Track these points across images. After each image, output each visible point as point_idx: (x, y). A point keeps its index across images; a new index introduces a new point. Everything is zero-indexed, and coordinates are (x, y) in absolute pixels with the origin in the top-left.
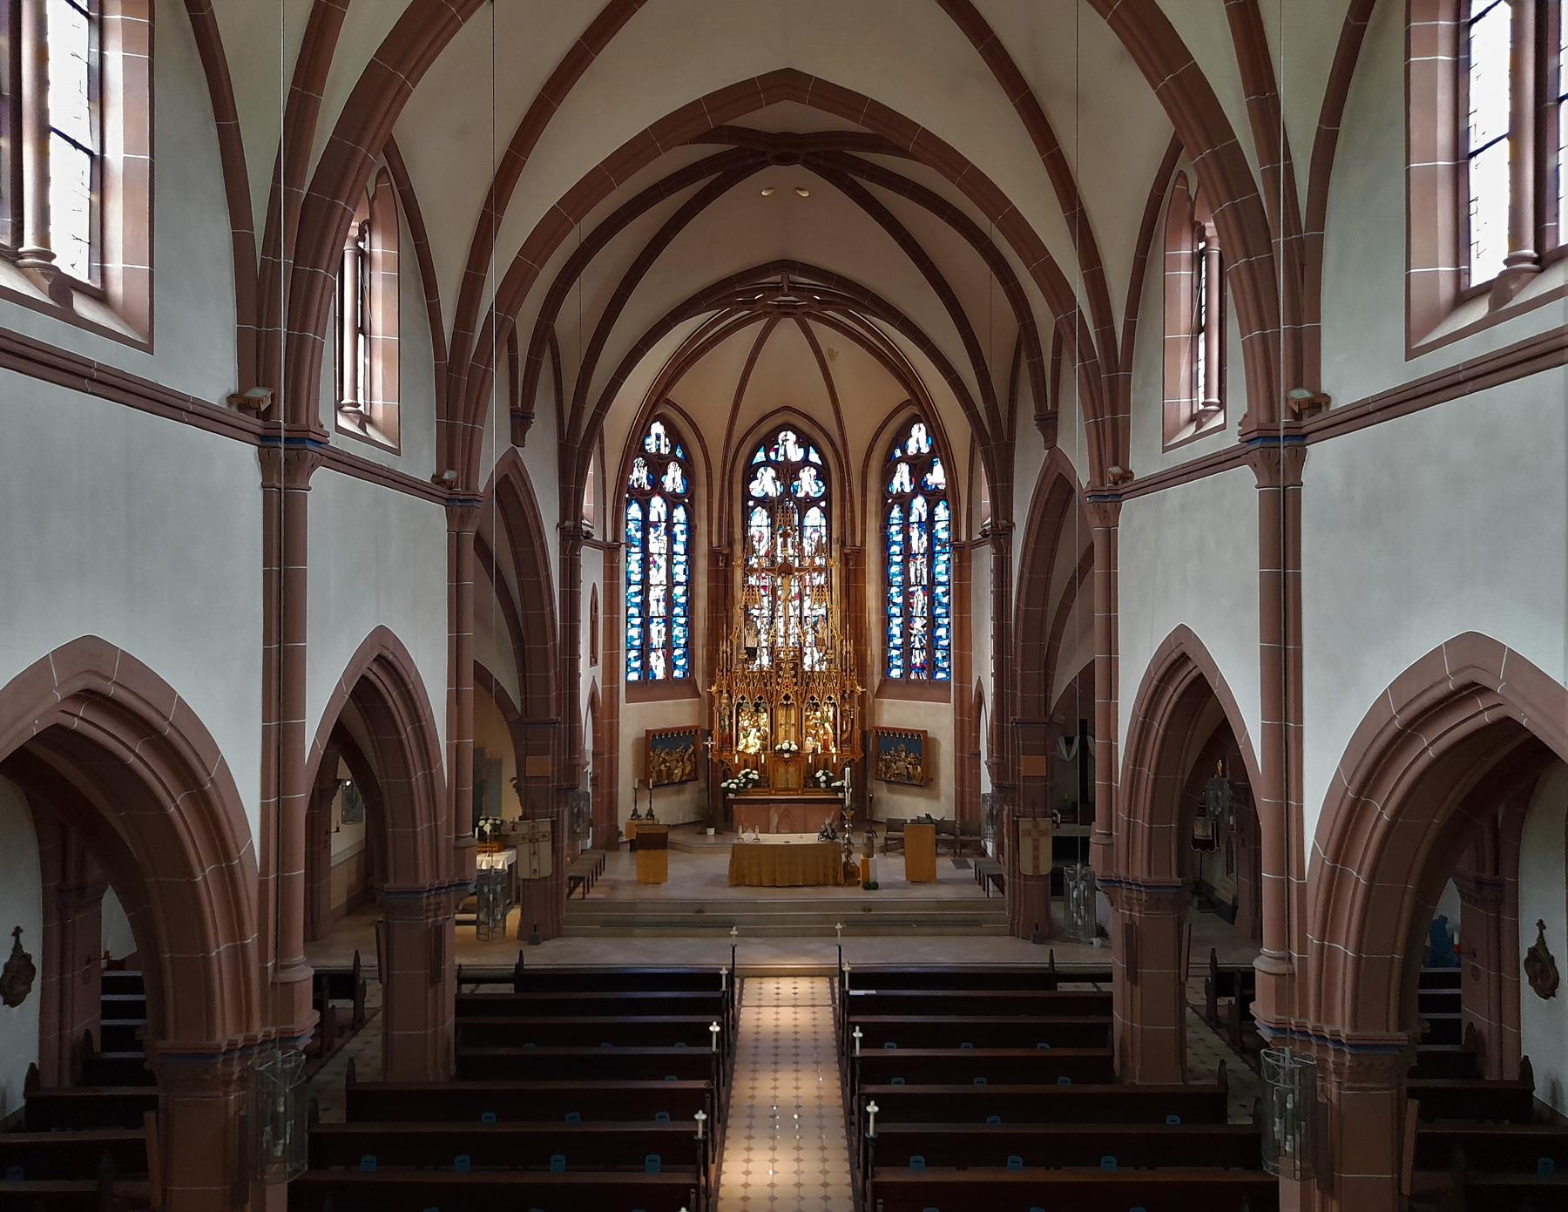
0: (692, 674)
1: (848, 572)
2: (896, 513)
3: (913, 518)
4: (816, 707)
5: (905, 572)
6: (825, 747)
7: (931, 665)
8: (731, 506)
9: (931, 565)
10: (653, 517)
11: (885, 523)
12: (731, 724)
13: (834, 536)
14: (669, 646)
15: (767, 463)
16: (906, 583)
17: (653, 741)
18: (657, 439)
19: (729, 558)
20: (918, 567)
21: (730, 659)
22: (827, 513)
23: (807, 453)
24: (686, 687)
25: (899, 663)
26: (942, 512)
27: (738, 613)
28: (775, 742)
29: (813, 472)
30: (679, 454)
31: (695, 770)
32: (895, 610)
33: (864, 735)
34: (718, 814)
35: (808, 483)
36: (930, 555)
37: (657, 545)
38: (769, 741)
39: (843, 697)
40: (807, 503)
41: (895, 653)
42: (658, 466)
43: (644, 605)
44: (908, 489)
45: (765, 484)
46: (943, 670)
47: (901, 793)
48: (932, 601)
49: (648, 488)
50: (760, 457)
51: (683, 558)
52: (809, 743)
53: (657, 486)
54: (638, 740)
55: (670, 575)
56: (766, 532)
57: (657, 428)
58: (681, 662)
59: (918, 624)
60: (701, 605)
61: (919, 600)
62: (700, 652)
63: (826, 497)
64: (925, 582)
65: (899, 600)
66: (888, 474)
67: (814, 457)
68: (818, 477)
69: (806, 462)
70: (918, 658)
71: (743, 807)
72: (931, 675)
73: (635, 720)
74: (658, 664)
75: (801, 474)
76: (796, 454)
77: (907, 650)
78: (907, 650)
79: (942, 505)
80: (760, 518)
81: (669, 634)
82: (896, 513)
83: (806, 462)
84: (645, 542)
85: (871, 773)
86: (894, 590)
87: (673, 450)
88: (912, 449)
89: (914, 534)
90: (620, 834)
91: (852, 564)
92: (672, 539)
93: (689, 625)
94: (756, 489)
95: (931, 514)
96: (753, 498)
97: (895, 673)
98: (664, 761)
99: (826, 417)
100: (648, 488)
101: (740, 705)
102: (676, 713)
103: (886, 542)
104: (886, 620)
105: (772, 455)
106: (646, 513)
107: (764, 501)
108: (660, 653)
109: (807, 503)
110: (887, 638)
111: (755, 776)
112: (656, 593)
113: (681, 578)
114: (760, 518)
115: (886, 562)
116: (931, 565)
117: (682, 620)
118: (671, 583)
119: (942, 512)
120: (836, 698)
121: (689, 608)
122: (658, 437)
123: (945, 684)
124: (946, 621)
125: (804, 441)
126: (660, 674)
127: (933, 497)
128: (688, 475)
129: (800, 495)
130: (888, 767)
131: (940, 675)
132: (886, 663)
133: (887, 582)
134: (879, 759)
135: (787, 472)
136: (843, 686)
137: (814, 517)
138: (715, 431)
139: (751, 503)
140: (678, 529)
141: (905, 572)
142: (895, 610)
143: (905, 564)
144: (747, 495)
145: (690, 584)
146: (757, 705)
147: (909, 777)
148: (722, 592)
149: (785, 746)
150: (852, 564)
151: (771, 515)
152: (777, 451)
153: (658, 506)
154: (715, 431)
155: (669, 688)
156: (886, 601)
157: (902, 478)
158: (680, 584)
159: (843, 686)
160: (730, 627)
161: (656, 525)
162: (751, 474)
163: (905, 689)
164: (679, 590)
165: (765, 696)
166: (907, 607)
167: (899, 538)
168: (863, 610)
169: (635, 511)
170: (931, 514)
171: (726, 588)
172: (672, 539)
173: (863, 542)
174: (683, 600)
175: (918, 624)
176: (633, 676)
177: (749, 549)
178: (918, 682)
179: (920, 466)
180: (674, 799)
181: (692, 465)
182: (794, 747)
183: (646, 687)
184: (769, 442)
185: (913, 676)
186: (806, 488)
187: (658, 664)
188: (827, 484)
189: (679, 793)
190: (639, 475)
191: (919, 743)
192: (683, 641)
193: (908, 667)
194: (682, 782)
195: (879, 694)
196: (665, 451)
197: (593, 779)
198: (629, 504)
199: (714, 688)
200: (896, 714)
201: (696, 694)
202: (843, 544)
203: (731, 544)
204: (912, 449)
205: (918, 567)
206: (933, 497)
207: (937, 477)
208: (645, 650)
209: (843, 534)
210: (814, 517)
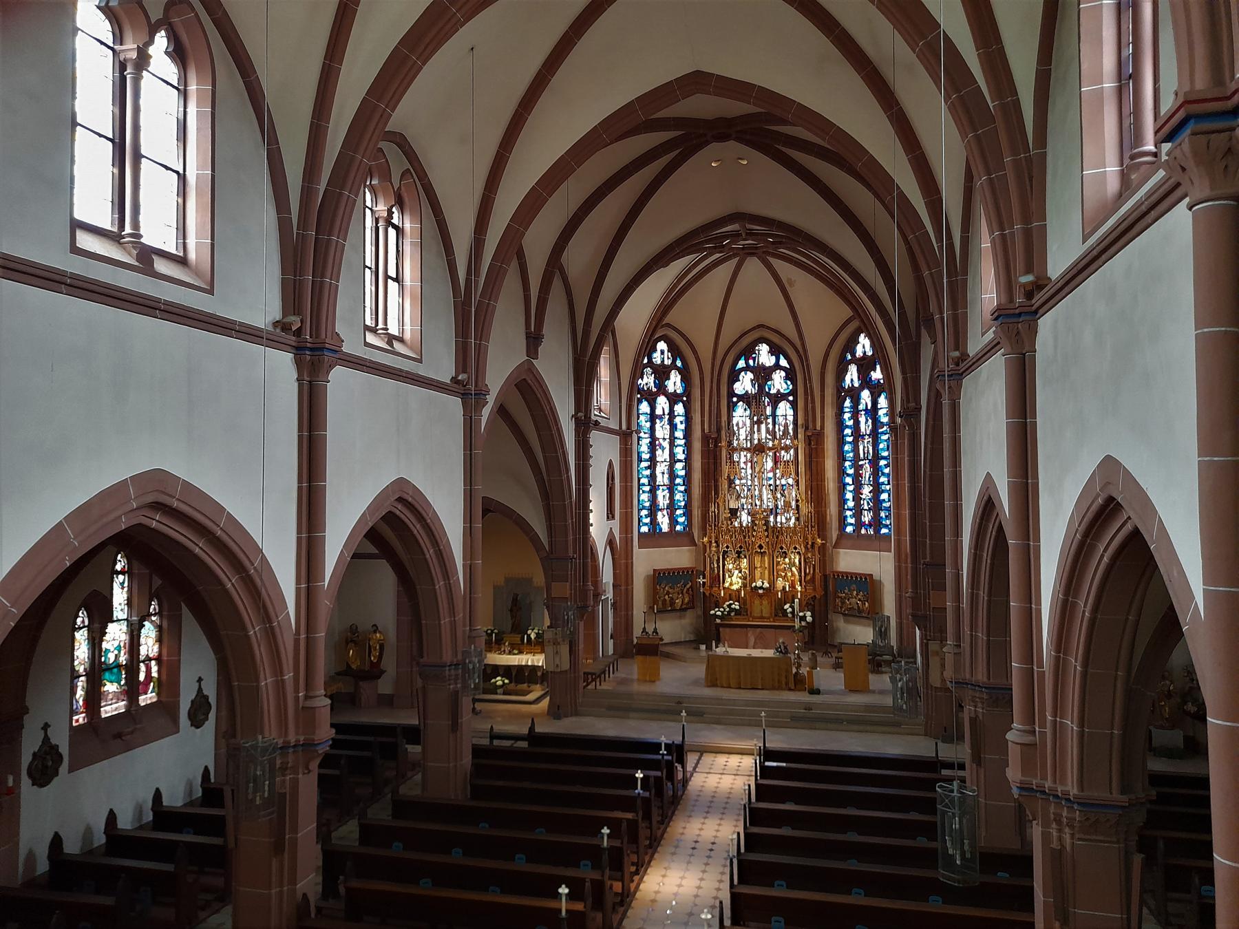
0: (691, 529)
1: (811, 449)
2: (848, 403)
3: (861, 407)
4: (785, 555)
5: (856, 450)
6: (793, 586)
7: (876, 523)
8: (719, 402)
10: (659, 412)
11: (840, 411)
13: (800, 422)
14: (672, 507)
15: (747, 368)
16: (857, 458)
17: (659, 578)
19: (717, 440)
20: (865, 446)
21: (717, 517)
22: (794, 405)
24: (685, 538)
27: (725, 485)
28: (753, 580)
29: (783, 374)
30: (679, 363)
31: (692, 601)
32: (849, 480)
33: (825, 577)
34: (708, 633)
35: (778, 382)
36: (875, 435)
37: (662, 431)
38: (748, 579)
39: (806, 547)
40: (777, 399)
41: (849, 513)
42: (662, 373)
43: (653, 477)
44: (856, 385)
45: (745, 384)
46: (886, 526)
47: (854, 623)
48: (876, 471)
49: (654, 390)
50: (741, 364)
51: (683, 442)
52: (780, 583)
53: (661, 389)
54: (648, 576)
55: (672, 454)
57: (662, 345)
58: (681, 520)
59: (866, 491)
60: (697, 476)
61: (867, 471)
62: (696, 513)
63: (793, 392)
65: (851, 471)
66: (842, 372)
67: (783, 362)
68: (787, 378)
69: (777, 366)
70: (867, 517)
71: (728, 630)
72: (877, 531)
73: (645, 561)
74: (664, 521)
77: (858, 511)
78: (858, 511)
79: (883, 396)
82: (848, 403)
83: (777, 366)
84: (652, 429)
85: (830, 607)
86: (847, 464)
88: (859, 352)
89: (862, 419)
91: (814, 442)
92: (673, 427)
93: (688, 491)
94: (739, 388)
96: (737, 395)
97: (849, 529)
98: (668, 593)
99: (791, 332)
100: (654, 390)
101: (725, 552)
102: (678, 558)
103: (840, 425)
104: (842, 487)
105: (751, 362)
106: (653, 408)
107: (745, 398)
109: (777, 399)
111: (736, 606)
112: (661, 468)
113: (681, 456)
115: (841, 442)
117: (682, 488)
118: (673, 460)
119: (883, 402)
121: (688, 479)
122: (662, 352)
123: (887, 536)
124: (888, 487)
125: (775, 351)
126: (665, 527)
128: (686, 379)
129: (773, 391)
130: (843, 603)
131: (884, 531)
132: (842, 522)
133: (841, 457)
134: (836, 597)
135: (763, 375)
136: (806, 538)
137: (784, 408)
138: (705, 345)
139: (735, 399)
140: (678, 420)
141: (856, 450)
142: (849, 480)
143: (855, 444)
144: (731, 393)
145: (688, 460)
146: (739, 553)
147: (860, 611)
149: (759, 584)
150: (814, 442)
152: (754, 359)
153: (662, 403)
154: (705, 345)
155: (672, 538)
156: (842, 472)
157: (852, 376)
158: (680, 461)
159: (806, 538)
160: (717, 493)
162: (734, 377)
163: (857, 542)
164: (679, 466)
165: (744, 545)
166: (857, 478)
167: (850, 423)
168: (823, 480)
169: (645, 407)
170: (875, 403)
172: (673, 427)
173: (822, 427)
174: (683, 473)
175: (866, 491)
176: (645, 529)
177: (732, 433)
178: (867, 536)
180: (677, 622)
181: (689, 372)
182: (766, 585)
183: (654, 537)
184: (749, 352)
185: (863, 531)
186: (778, 386)
187: (664, 521)
188: (794, 383)
189: (680, 618)
190: (648, 381)
191: (867, 584)
193: (859, 524)
194: (682, 610)
195: (837, 546)
196: (667, 362)
197: (614, 605)
198: (640, 401)
199: (706, 539)
200: (850, 561)
202: (807, 429)
203: (719, 430)
204: (859, 352)
205: (865, 446)
207: (877, 375)
208: (653, 510)
209: (806, 421)
210: (784, 408)
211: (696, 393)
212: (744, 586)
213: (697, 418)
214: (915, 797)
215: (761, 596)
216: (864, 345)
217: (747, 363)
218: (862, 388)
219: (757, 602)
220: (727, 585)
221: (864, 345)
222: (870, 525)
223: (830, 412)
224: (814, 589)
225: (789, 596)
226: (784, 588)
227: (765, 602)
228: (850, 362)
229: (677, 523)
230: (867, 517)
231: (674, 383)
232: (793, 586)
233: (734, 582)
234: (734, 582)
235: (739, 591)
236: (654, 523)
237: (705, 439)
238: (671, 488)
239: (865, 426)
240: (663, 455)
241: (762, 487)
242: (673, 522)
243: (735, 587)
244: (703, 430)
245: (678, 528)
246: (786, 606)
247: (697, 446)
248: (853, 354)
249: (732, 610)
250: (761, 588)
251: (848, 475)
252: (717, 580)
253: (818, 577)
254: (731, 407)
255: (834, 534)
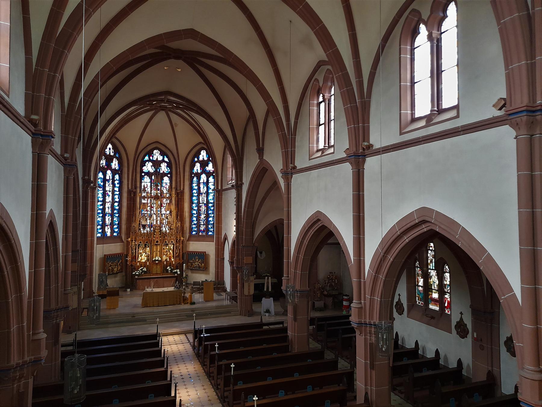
0: (120, 234)
2: (195, 179)
3: (201, 181)
5: (198, 199)
6: (170, 259)
7: (207, 230)
8: (136, 175)
9: (207, 197)
10: (107, 178)
11: (191, 183)
12: (136, 252)
14: (112, 224)
15: (149, 160)
16: (199, 202)
17: (106, 259)
18: (109, 150)
19: (135, 194)
22: (171, 179)
23: (164, 158)
25: (196, 229)
26: (211, 179)
29: (166, 164)
31: (122, 269)
32: (195, 212)
34: (131, 283)
35: (164, 168)
37: (108, 188)
38: (150, 258)
42: (109, 159)
43: (104, 209)
44: (199, 171)
45: (148, 167)
47: (196, 273)
48: (208, 208)
50: (147, 158)
51: (118, 193)
52: (164, 258)
53: (109, 166)
54: (100, 258)
55: (113, 199)
56: (149, 184)
57: (110, 146)
59: (203, 216)
60: (124, 210)
61: (203, 208)
62: (124, 227)
63: (170, 173)
64: (205, 202)
65: (196, 208)
66: (193, 166)
67: (166, 159)
68: (167, 166)
69: (163, 161)
70: (202, 228)
71: (141, 281)
72: (207, 233)
74: (108, 231)
75: (161, 165)
76: (160, 158)
78: (198, 225)
80: (147, 179)
81: (112, 220)
82: (195, 179)
83: (163, 161)
84: (104, 187)
86: (194, 205)
87: (115, 154)
88: (201, 158)
89: (202, 186)
90: (94, 293)
92: (114, 186)
93: (120, 217)
94: (145, 169)
95: (208, 180)
96: (144, 172)
98: (111, 266)
99: (171, 145)
101: (139, 245)
102: (115, 248)
103: (191, 189)
105: (151, 158)
107: (148, 174)
108: (109, 227)
109: (165, 174)
110: (191, 221)
111: (145, 269)
112: (108, 205)
113: (117, 200)
114: (147, 179)
115: (191, 195)
116: (207, 197)
117: (117, 215)
118: (113, 201)
119: (211, 179)
120: (174, 242)
121: (120, 211)
122: (110, 149)
123: (212, 236)
124: (212, 215)
125: (162, 154)
126: (109, 234)
127: (208, 174)
128: (120, 164)
129: (161, 172)
130: (192, 265)
132: (191, 229)
133: (192, 202)
135: (157, 164)
136: (177, 238)
137: (166, 180)
138: (131, 147)
139: (143, 174)
140: (116, 182)
141: (198, 199)
142: (195, 212)
143: (198, 196)
144: (142, 171)
145: (120, 202)
146: (145, 245)
147: (199, 267)
148: (132, 205)
149: (157, 258)
151: (151, 178)
152: (153, 156)
154: (131, 147)
156: (191, 209)
157: (197, 168)
158: (116, 202)
159: (177, 238)
161: (108, 180)
162: (143, 164)
163: (198, 238)
164: (116, 204)
165: (148, 241)
166: (199, 210)
167: (196, 188)
168: (183, 212)
169: (101, 175)
170: (208, 180)
171: (134, 204)
172: (114, 186)
173: (184, 189)
174: (117, 208)
175: (203, 216)
176: (99, 235)
178: (202, 236)
179: (204, 164)
180: (113, 279)
183: (104, 238)
184: (150, 153)
186: (163, 170)
187: (108, 231)
189: (115, 277)
190: (103, 162)
191: (203, 256)
192: (117, 223)
193: (199, 231)
194: (117, 273)
195: (189, 240)
196: (112, 154)
199: (129, 239)
200: (195, 246)
201: (123, 242)
202: (176, 189)
203: (136, 188)
204: (201, 158)
205: (203, 198)
206: (208, 174)
207: (210, 168)
208: (104, 225)
211: (125, 170)
212: (148, 260)
213: (125, 182)
214: (117, 355)
215: (157, 264)
216: (203, 155)
217: (149, 158)
218: (202, 173)
219: (155, 267)
220: (139, 260)
221: (203, 155)
222: (204, 231)
223: (187, 183)
224: (180, 260)
225: (169, 264)
226: (166, 260)
227: (159, 267)
228: (197, 162)
229: (114, 232)
230: (202, 228)
231: (115, 164)
232: (170, 259)
233: (143, 258)
234: (143, 258)
235: (145, 262)
236: (104, 232)
237: (129, 192)
238: (112, 215)
239: (203, 189)
240: (109, 199)
241: (157, 215)
242: (112, 231)
243: (144, 261)
244: (128, 188)
245: (115, 234)
246: (168, 268)
247: (125, 195)
248: (198, 159)
249: (143, 271)
250: (158, 260)
251: (194, 210)
252: (135, 258)
253: (181, 254)
254: (142, 178)
255: (187, 235)
